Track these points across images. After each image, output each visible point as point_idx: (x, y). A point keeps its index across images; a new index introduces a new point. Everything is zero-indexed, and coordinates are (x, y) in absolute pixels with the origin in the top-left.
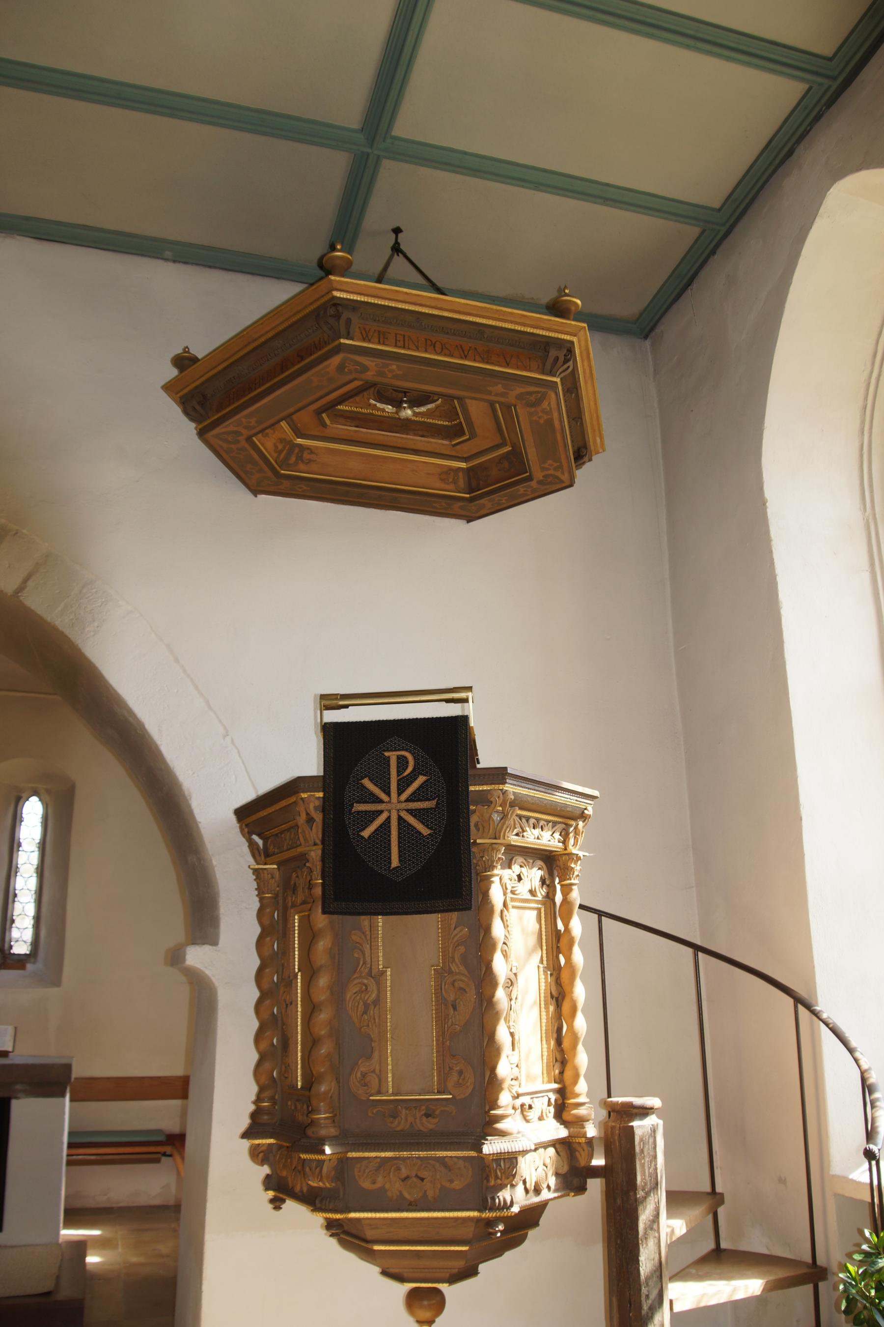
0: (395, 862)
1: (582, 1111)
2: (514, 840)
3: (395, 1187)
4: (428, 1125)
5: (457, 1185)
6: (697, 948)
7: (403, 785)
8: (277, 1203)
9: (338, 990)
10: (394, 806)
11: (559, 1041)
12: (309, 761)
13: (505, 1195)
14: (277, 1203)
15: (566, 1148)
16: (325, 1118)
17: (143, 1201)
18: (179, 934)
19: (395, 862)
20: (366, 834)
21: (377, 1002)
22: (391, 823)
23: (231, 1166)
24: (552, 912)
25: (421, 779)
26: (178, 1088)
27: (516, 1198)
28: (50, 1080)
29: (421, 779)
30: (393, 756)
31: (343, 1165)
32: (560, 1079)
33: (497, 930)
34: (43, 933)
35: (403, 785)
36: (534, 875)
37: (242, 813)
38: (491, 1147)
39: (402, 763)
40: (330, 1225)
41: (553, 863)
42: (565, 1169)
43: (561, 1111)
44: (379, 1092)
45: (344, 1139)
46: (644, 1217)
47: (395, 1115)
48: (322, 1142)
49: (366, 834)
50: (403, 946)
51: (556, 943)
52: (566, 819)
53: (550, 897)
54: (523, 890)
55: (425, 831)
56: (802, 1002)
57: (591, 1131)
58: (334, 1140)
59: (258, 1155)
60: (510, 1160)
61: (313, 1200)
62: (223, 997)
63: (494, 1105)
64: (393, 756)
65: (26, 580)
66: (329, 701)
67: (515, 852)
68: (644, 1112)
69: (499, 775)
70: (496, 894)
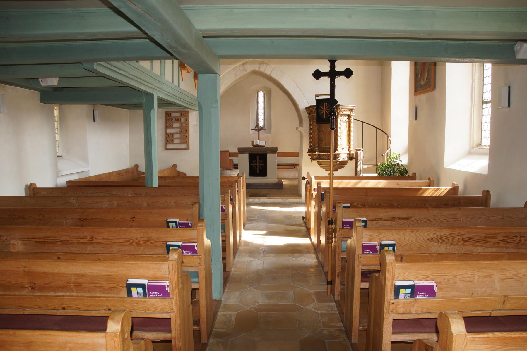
2: (341, 113)
3: (325, 157)
6: (377, 128)
8: (312, 161)
9: (318, 133)
10: (324, 110)
12: (314, 103)
13: (339, 159)
14: (312, 161)
15: (349, 154)
17: (290, 177)
18: (298, 125)
22: (324, 113)
23: (305, 157)
24: (349, 123)
26: (297, 155)
27: (340, 159)
28: (274, 150)
31: (319, 155)
33: (339, 126)
34: (266, 122)
36: (346, 118)
37: (306, 108)
38: (336, 152)
40: (318, 162)
41: (349, 116)
43: (349, 149)
45: (319, 151)
46: (359, 163)
50: (325, 127)
51: (349, 127)
52: (351, 110)
53: (349, 121)
54: (344, 120)
56: (388, 137)
57: (352, 152)
59: (310, 155)
60: (339, 154)
61: (315, 159)
62: (304, 134)
66: (317, 96)
67: (342, 115)
68: (360, 150)
69: (339, 105)
70: (339, 121)
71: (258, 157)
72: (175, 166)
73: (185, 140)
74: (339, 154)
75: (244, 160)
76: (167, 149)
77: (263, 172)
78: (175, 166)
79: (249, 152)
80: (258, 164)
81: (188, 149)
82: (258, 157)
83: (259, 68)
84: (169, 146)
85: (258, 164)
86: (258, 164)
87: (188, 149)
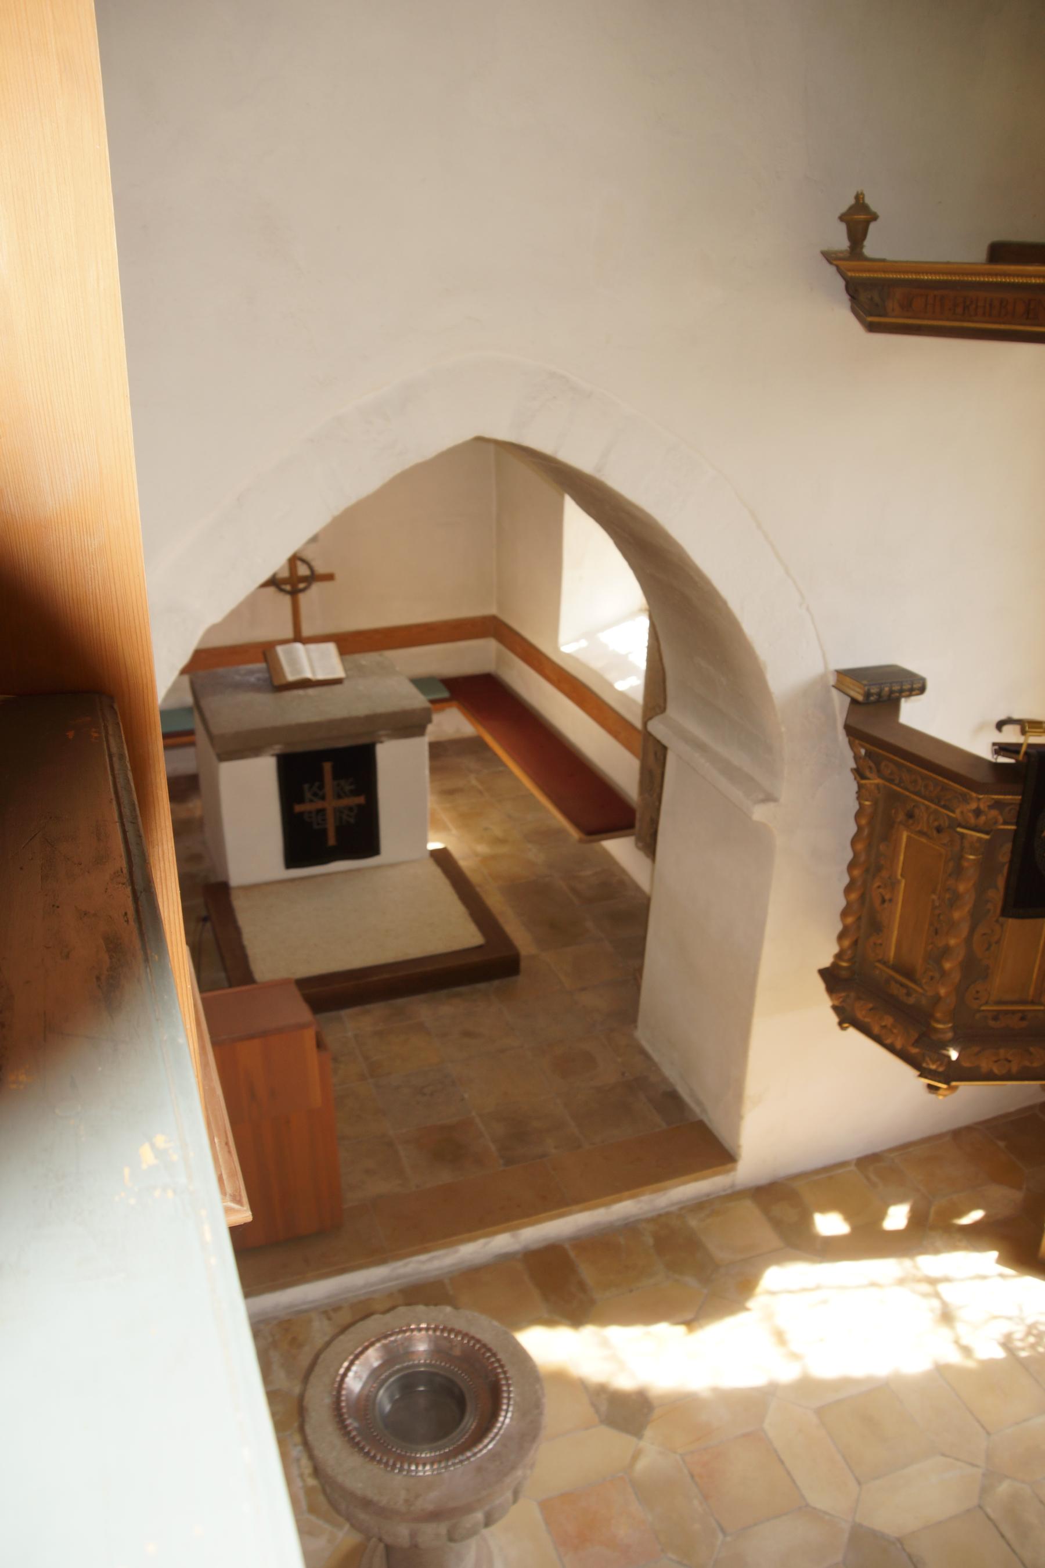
5: (1035, 1065)
16: (938, 1022)
21: (997, 942)
44: (986, 1003)
48: (945, 1045)
58: (953, 1043)
71: (327, 767)
77: (361, 837)
79: (278, 749)
80: (331, 804)
82: (327, 767)
85: (331, 804)
86: (331, 804)
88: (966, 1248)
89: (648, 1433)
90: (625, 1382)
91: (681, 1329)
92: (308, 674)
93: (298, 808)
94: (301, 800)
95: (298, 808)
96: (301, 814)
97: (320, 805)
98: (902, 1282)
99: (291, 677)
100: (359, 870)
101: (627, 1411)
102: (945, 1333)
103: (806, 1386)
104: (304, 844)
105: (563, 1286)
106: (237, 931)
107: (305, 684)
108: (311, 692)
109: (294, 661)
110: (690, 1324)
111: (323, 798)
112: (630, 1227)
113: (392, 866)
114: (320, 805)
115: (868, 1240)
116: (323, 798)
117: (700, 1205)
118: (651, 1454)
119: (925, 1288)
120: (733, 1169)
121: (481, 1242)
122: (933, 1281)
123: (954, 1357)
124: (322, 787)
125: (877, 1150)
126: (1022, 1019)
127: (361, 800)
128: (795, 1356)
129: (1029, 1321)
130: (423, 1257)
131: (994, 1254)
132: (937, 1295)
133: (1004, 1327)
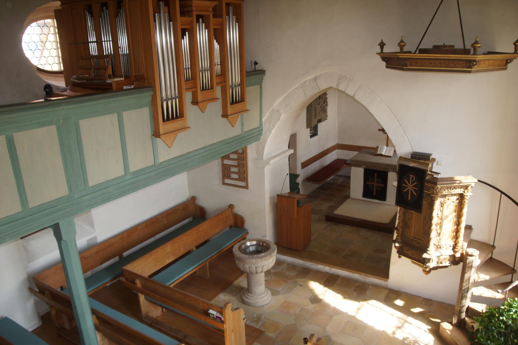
0: (409, 199)
1: (456, 250)
4: (418, 245)
7: (413, 183)
11: (456, 234)
19: (409, 199)
20: (405, 191)
25: (416, 183)
29: (416, 183)
30: (411, 176)
32: (455, 242)
35: (413, 183)
38: (425, 256)
39: (413, 178)
42: (452, 260)
47: (412, 241)
49: (405, 191)
55: (415, 194)
63: (428, 248)
64: (411, 176)
65: (356, 92)
68: (472, 256)
72: (231, 207)
73: (243, 176)
74: (429, 260)
75: (357, 176)
76: (224, 184)
77: (382, 196)
78: (231, 207)
79: (365, 167)
80: (375, 184)
81: (246, 187)
82: (376, 174)
83: (338, 85)
84: (227, 181)
87: (246, 187)
88: (425, 323)
89: (314, 305)
90: (321, 297)
91: (342, 297)
92: (383, 154)
93: (367, 183)
94: (368, 181)
95: (367, 183)
96: (368, 184)
97: (373, 183)
98: (399, 318)
99: (378, 153)
100: (380, 203)
101: (315, 300)
102: (394, 329)
103: (353, 317)
104: (368, 193)
105: (330, 281)
106: (342, 204)
107: (381, 155)
108: (382, 157)
109: (382, 149)
110: (345, 298)
111: (374, 182)
112: (356, 281)
113: (388, 205)
114: (373, 183)
115: (405, 310)
116: (374, 182)
117: (377, 286)
118: (311, 307)
119: (403, 322)
120: (387, 281)
121: (323, 266)
122: (406, 321)
123: (390, 332)
124: (374, 179)
125: (433, 299)
126: (418, 244)
127: (383, 185)
128: (357, 313)
129: (417, 339)
130: (311, 263)
131: (430, 328)
132: (403, 324)
133: (409, 336)
